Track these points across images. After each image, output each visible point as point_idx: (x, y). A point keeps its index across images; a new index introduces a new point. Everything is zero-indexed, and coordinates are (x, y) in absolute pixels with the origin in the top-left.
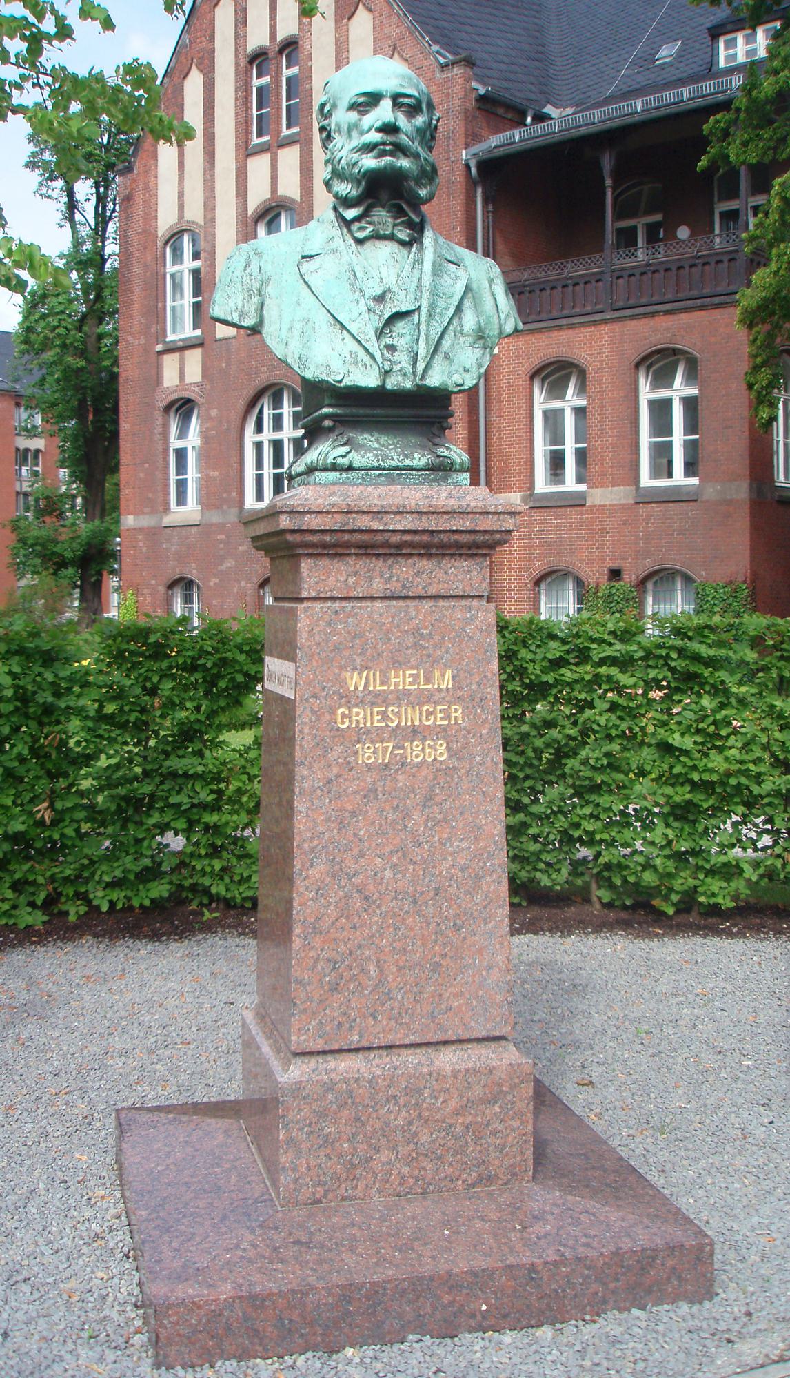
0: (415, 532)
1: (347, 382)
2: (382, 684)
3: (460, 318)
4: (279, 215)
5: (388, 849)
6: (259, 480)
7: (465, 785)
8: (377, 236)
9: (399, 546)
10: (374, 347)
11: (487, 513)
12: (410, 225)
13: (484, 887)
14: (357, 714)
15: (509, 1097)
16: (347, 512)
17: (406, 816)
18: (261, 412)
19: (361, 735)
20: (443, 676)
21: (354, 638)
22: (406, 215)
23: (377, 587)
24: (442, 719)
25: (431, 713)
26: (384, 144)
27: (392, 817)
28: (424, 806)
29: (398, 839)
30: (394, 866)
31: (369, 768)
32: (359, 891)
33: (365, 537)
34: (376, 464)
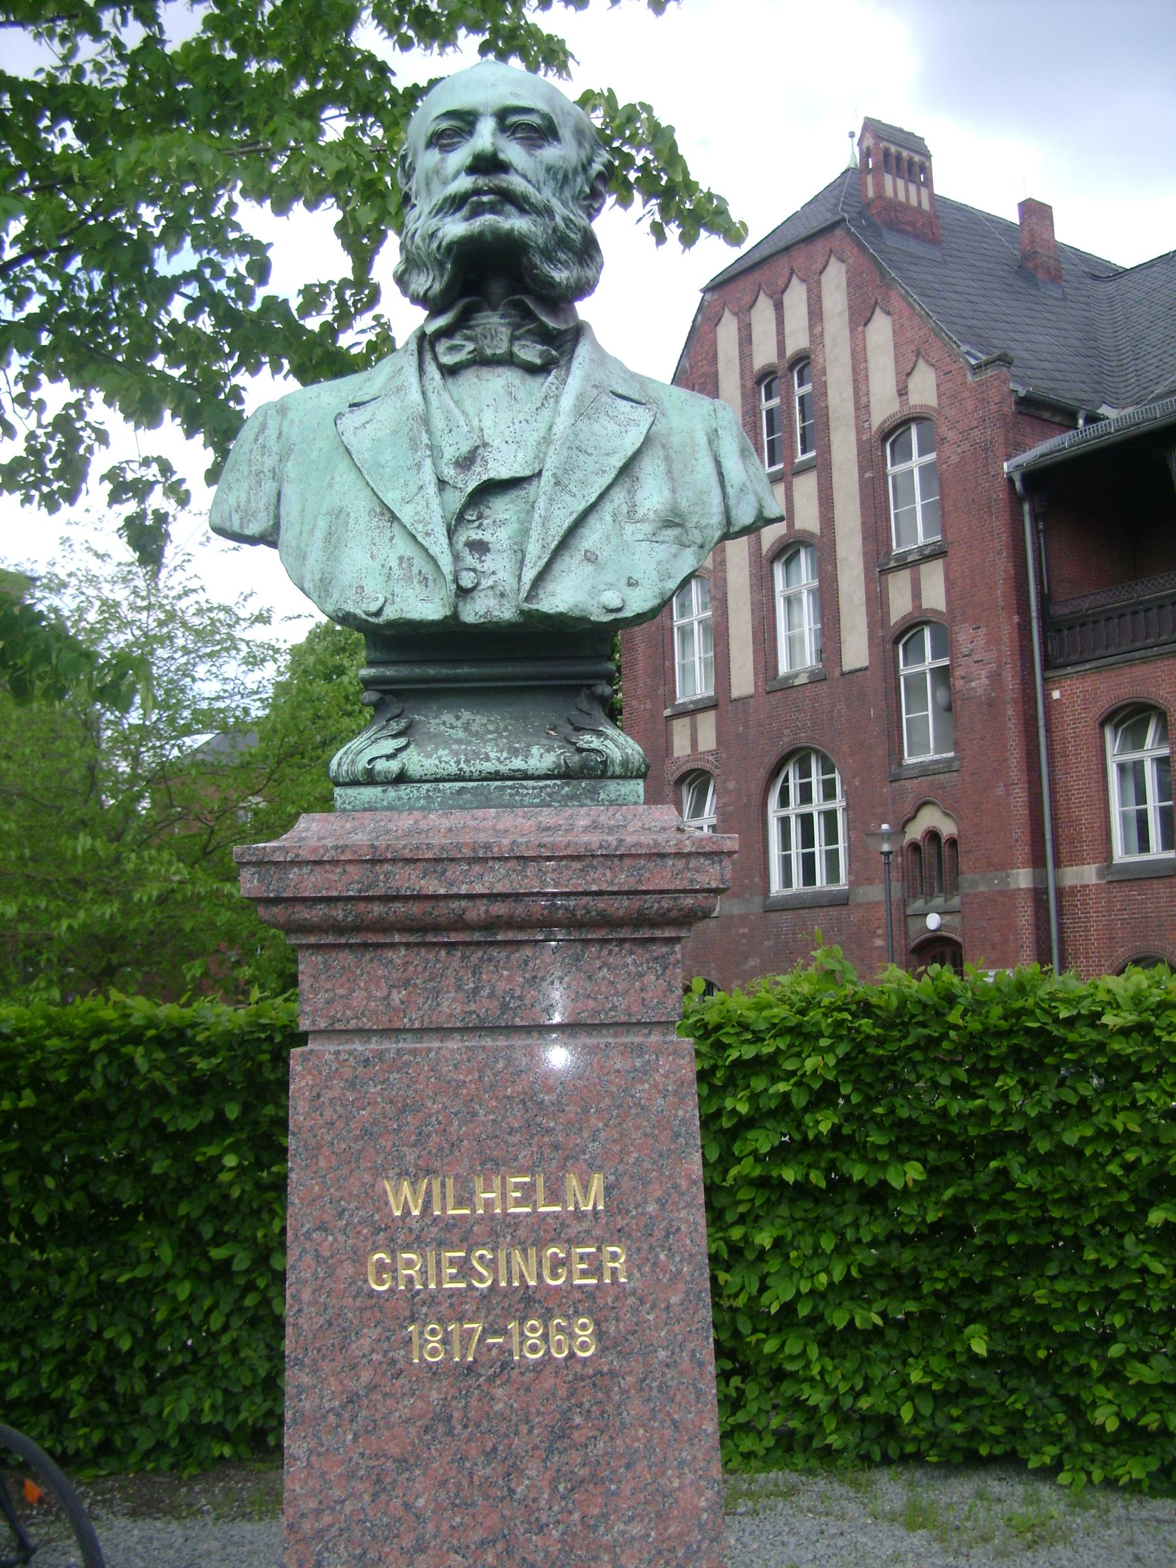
0: (517, 897)
1: (390, 614)
2: (459, 1203)
3: (631, 493)
4: (797, 552)
5: (476, 1536)
6: (786, 861)
7: (635, 1408)
8: (481, 361)
9: (491, 925)
10: (439, 545)
11: (663, 856)
12: (547, 337)
14: (409, 1264)
16: (373, 862)
17: (513, 1471)
18: (786, 779)
20: (586, 1187)
21: (402, 1111)
22: (536, 319)
23: (450, 1007)
24: (584, 1274)
25: (563, 1263)
26: (477, 192)
27: (482, 1472)
28: (550, 1451)
29: (494, 1519)
31: (434, 1372)
33: (415, 909)
34: (453, 769)
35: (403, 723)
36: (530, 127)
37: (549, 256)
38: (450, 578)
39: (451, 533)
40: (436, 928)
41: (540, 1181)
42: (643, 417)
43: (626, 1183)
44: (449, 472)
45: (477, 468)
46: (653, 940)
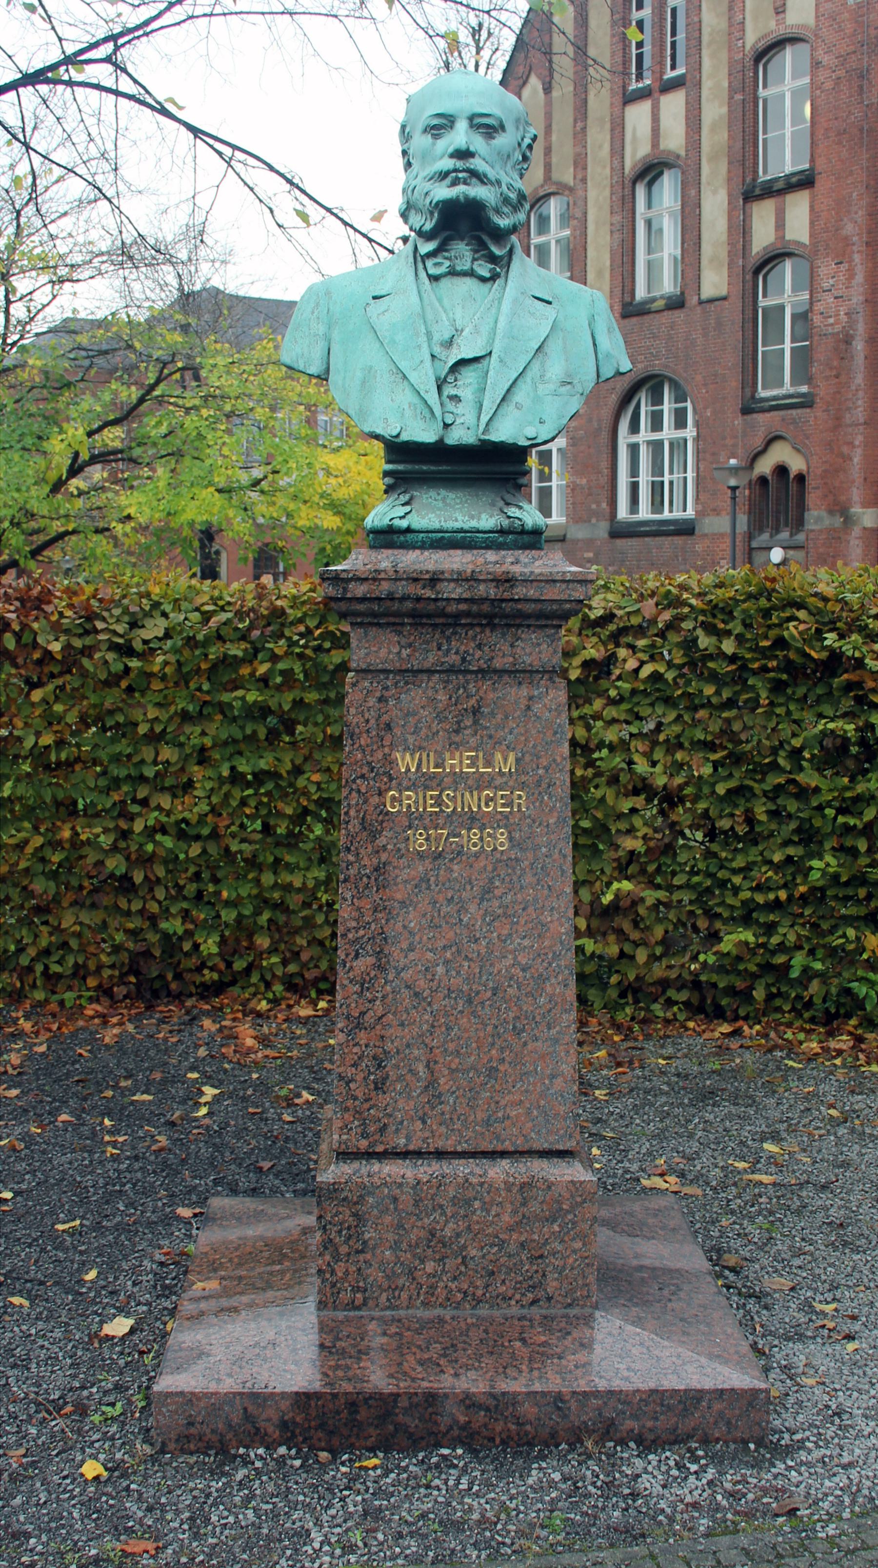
1: (404, 437)
2: (436, 767)
3: (543, 364)
4: (661, 173)
5: (440, 944)
6: (634, 488)
7: (529, 879)
8: (453, 273)
9: (458, 616)
10: (433, 398)
11: (554, 581)
12: (493, 259)
13: (549, 989)
15: (570, 1216)
16: (396, 580)
18: (638, 407)
19: (413, 820)
20: (505, 760)
21: (407, 715)
22: (488, 248)
24: (503, 805)
25: (492, 799)
26: (456, 170)
27: (445, 910)
28: (482, 899)
29: (451, 934)
30: (447, 962)
31: (421, 856)
32: (408, 987)
35: (407, 497)
36: (487, 126)
37: (497, 211)
38: (440, 418)
39: (439, 388)
40: (429, 616)
41: (481, 755)
42: (550, 312)
43: (528, 758)
44: (437, 350)
45: (455, 350)
46: (546, 626)
